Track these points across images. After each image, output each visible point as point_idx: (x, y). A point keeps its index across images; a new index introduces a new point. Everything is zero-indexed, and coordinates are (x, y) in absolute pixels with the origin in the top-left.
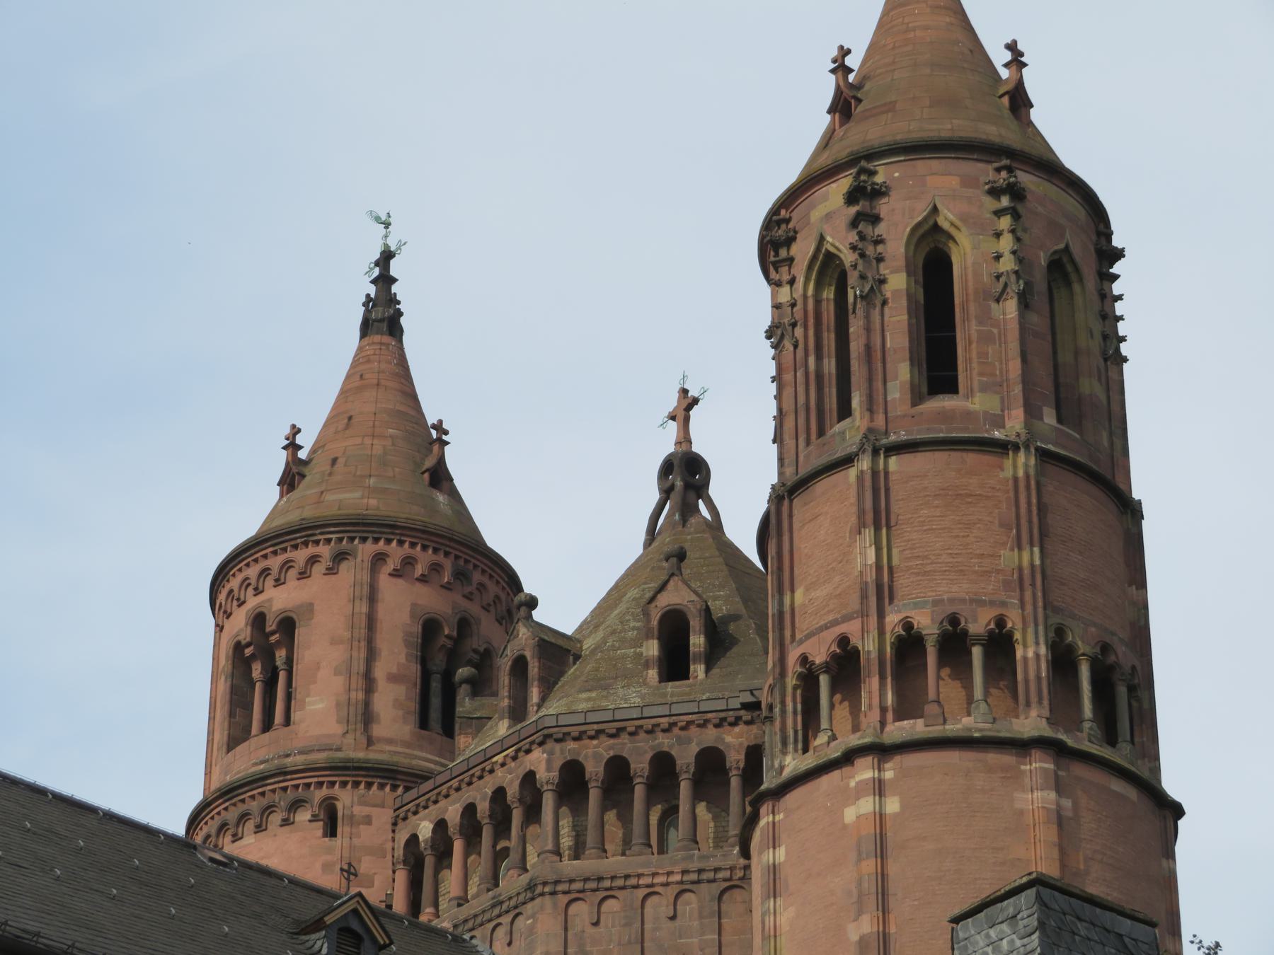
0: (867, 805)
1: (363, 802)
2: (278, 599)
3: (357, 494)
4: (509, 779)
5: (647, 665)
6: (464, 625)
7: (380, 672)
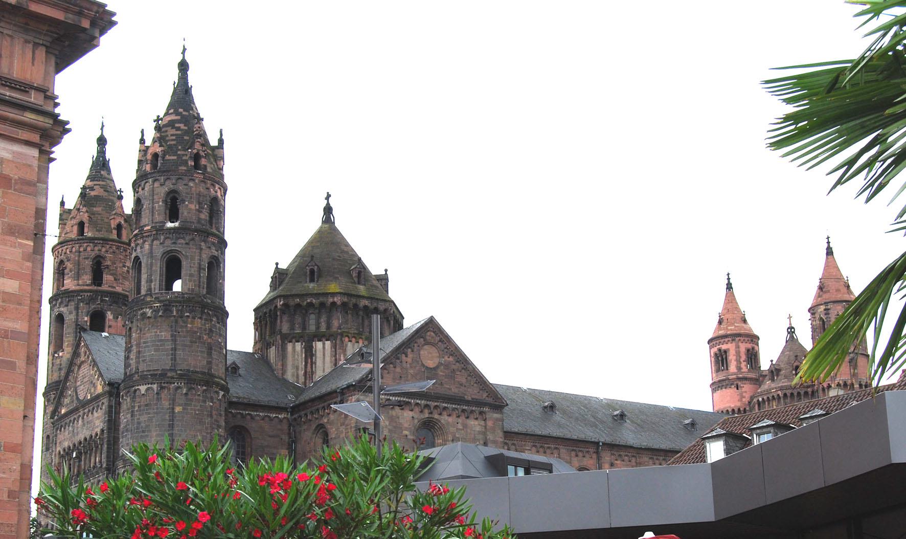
1: (742, 384)
2: (724, 347)
3: (733, 327)
6: (753, 348)
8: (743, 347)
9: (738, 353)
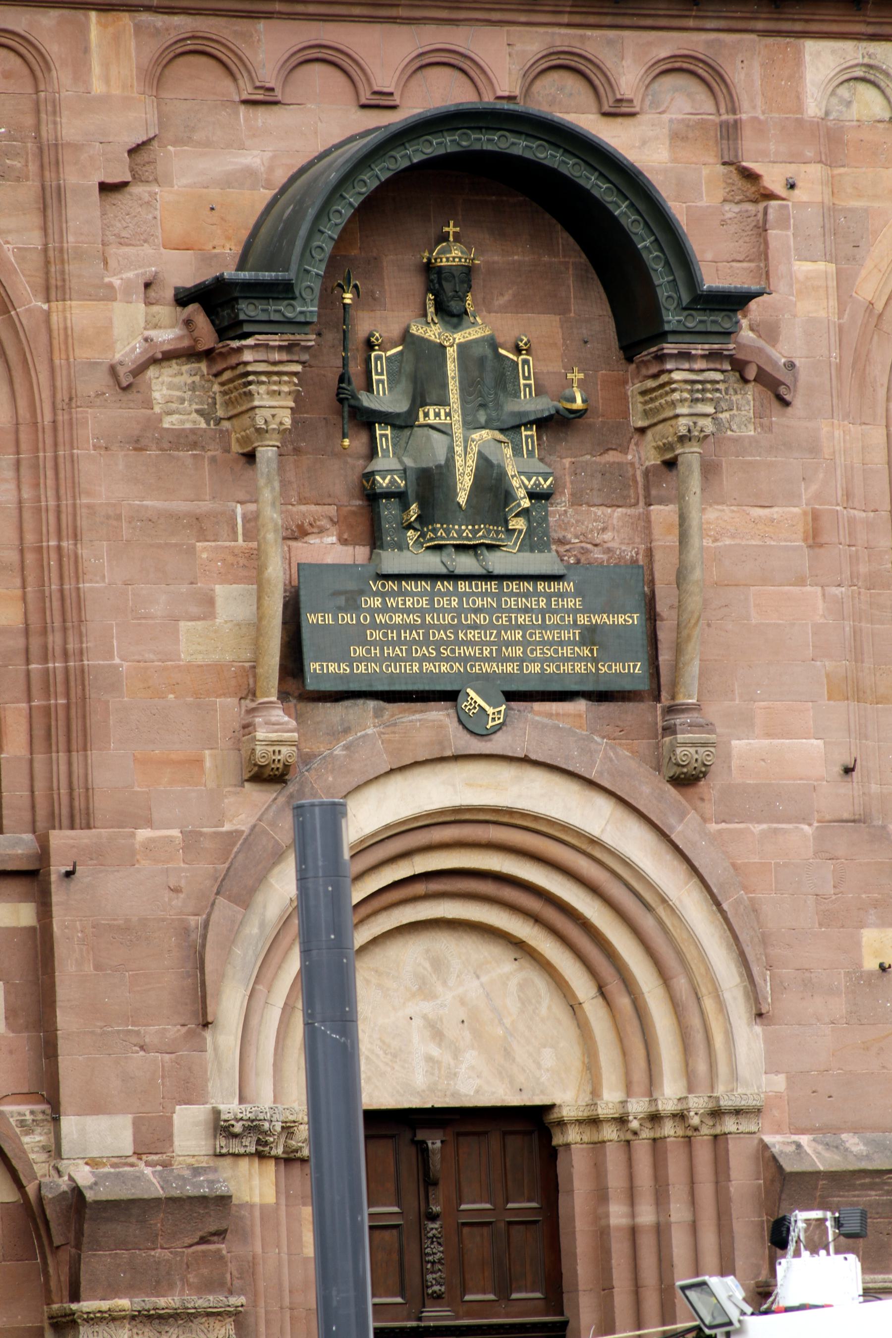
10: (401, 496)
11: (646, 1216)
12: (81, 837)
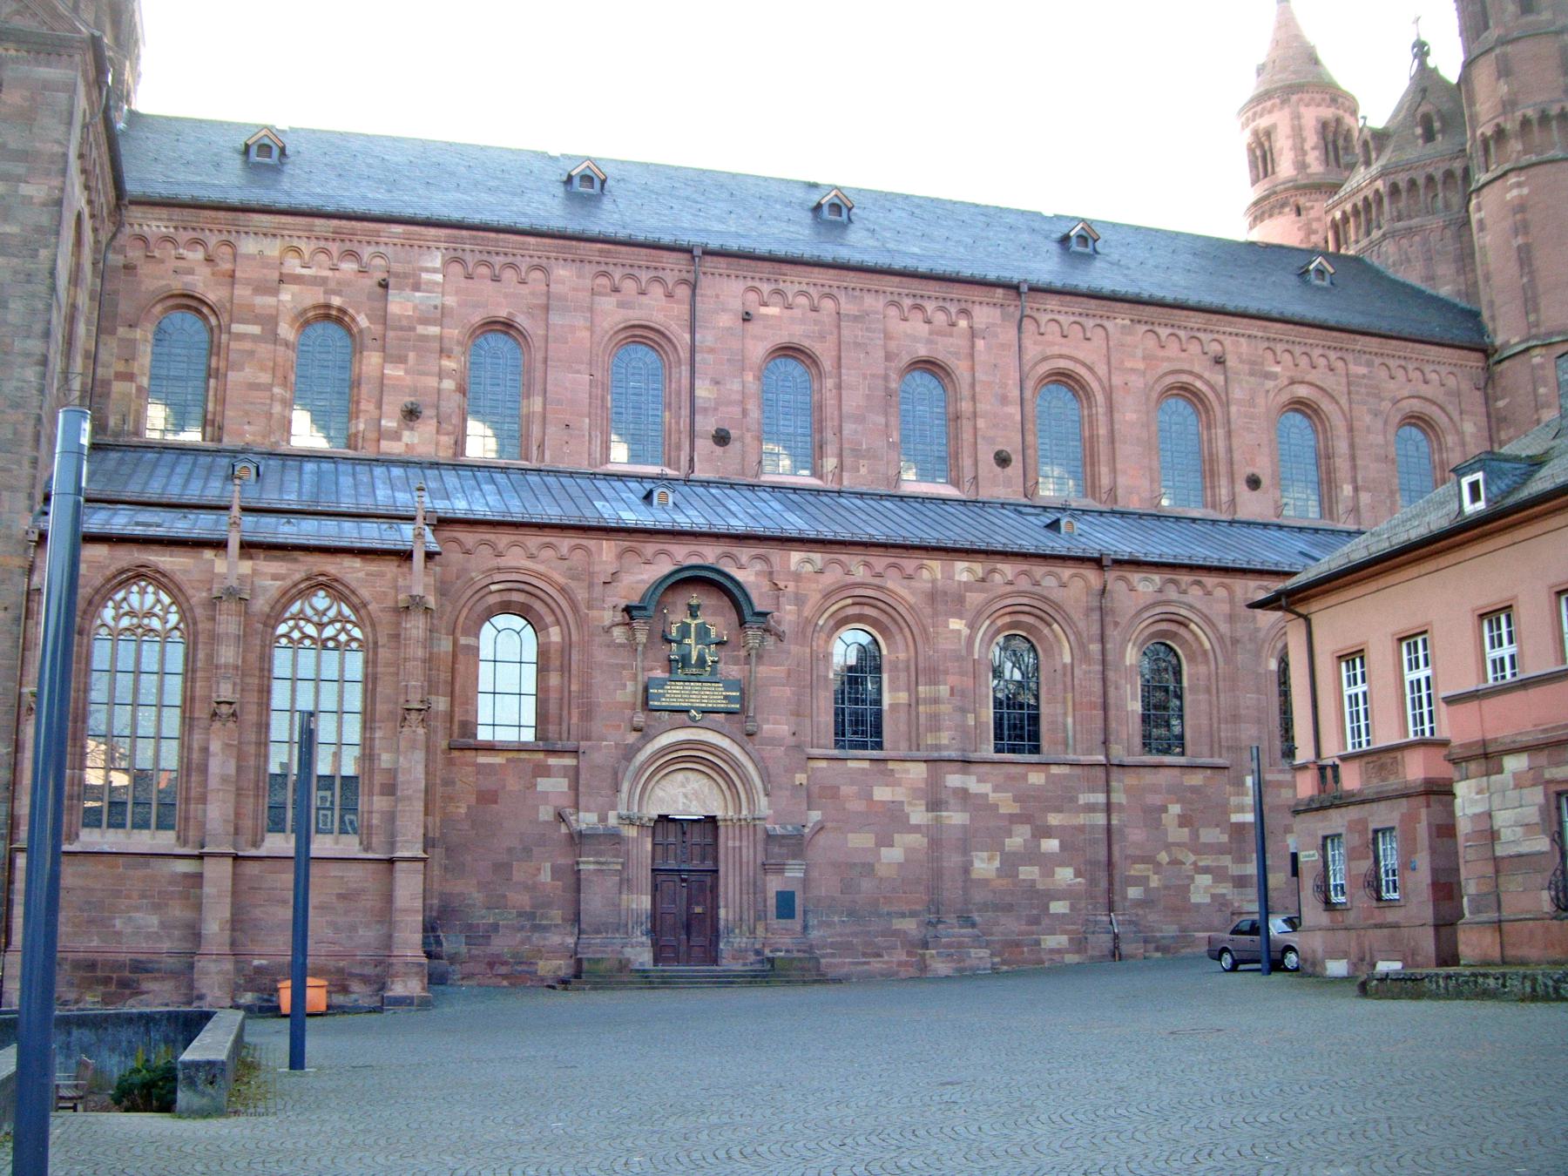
0: (1515, 192)
4: (1370, 193)
5: (1418, 138)
6: (1338, 121)
7: (1307, 146)
8: (1311, 116)
9: (1297, 133)
10: (677, 661)
11: (737, 844)
12: (589, 743)
